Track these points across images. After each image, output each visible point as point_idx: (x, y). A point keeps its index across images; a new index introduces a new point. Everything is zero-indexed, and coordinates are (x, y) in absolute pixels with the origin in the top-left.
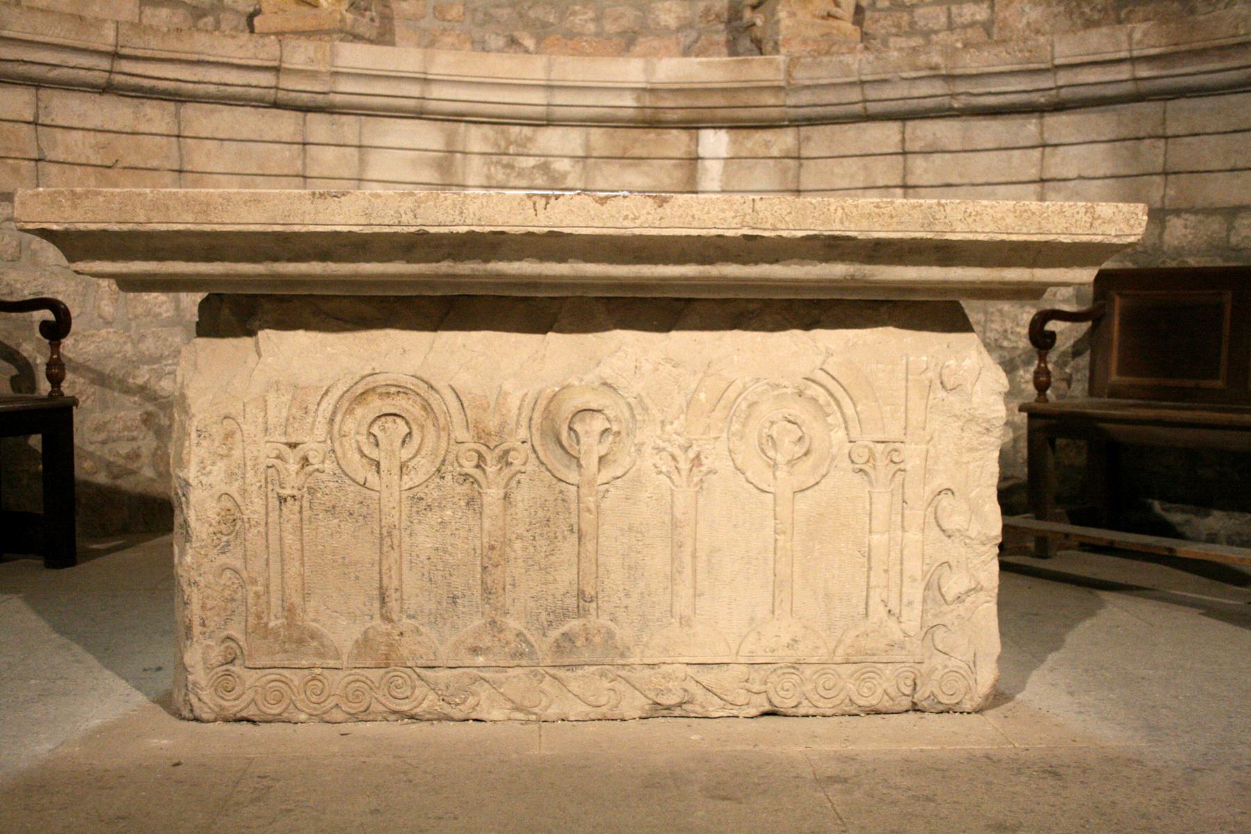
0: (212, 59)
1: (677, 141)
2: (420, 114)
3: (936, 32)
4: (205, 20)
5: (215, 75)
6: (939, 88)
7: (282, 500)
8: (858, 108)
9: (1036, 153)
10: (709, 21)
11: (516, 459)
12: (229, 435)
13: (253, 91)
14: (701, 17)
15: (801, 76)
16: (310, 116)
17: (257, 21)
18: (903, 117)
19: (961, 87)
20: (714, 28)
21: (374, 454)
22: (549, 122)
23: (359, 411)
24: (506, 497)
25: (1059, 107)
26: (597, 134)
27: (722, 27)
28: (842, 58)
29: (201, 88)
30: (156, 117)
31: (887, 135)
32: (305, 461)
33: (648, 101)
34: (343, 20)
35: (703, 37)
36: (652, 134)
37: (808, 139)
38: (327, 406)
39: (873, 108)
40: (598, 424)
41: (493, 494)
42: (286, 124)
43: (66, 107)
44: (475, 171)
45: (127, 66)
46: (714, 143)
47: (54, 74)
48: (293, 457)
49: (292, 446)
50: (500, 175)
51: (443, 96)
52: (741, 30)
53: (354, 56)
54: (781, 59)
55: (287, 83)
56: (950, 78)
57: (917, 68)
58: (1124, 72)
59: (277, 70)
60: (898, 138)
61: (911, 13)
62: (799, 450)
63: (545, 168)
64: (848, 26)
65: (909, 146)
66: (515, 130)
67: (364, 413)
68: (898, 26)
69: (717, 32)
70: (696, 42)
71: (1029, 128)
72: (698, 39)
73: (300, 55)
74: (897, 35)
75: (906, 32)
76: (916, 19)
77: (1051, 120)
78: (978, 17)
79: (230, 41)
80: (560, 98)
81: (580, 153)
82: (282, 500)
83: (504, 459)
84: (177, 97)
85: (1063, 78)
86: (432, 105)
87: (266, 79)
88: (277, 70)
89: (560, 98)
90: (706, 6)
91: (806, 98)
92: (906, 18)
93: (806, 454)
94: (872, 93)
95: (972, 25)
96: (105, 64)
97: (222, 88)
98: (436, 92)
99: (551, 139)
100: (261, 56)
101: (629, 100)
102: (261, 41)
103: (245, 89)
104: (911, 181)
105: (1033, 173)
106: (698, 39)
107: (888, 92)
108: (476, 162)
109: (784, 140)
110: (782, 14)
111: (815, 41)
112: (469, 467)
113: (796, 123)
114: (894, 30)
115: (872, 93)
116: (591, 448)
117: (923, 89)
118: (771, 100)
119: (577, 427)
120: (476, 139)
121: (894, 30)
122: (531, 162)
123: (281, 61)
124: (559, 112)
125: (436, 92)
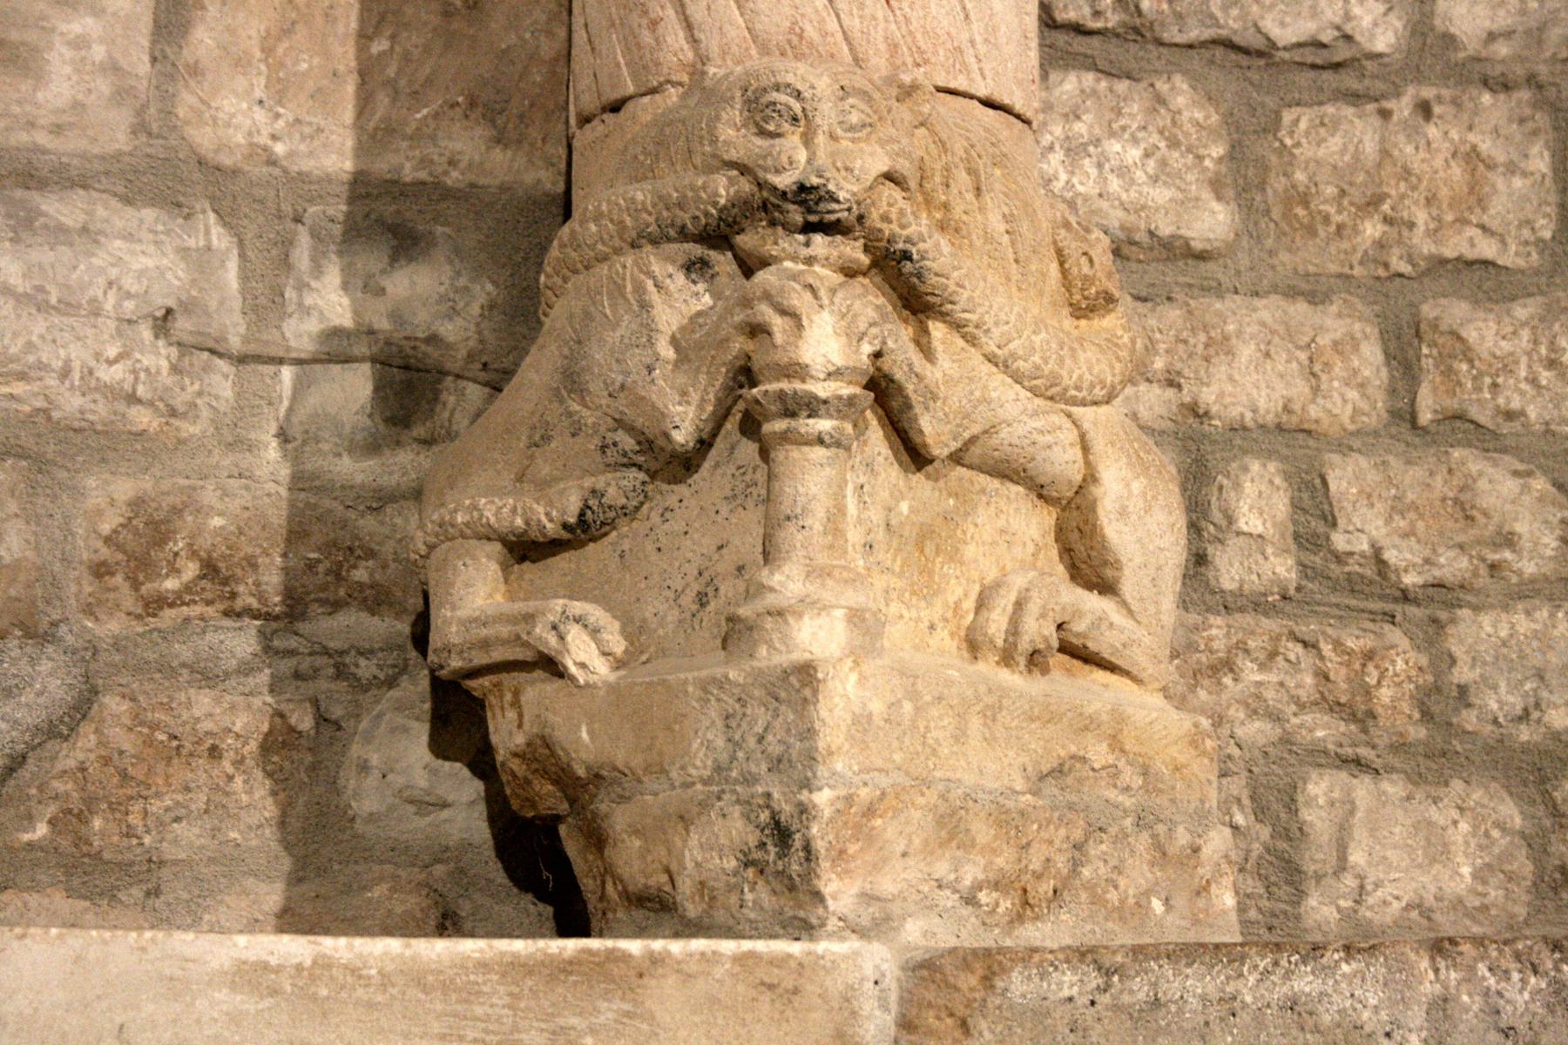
10: (155, 604)
14: (100, 570)
20: (183, 651)
27: (242, 642)
28: (1305, 983)
35: (113, 704)
52: (366, 669)
61: (1433, 634)
68: (1361, 716)
69: (207, 675)
70: (57, 730)
72: (82, 707)
74: (1358, 765)
75: (1401, 747)
76: (1463, 673)
90: (137, 503)
106: (82, 707)
111: (1008, 821)
114: (1324, 730)
121: (1324, 730)
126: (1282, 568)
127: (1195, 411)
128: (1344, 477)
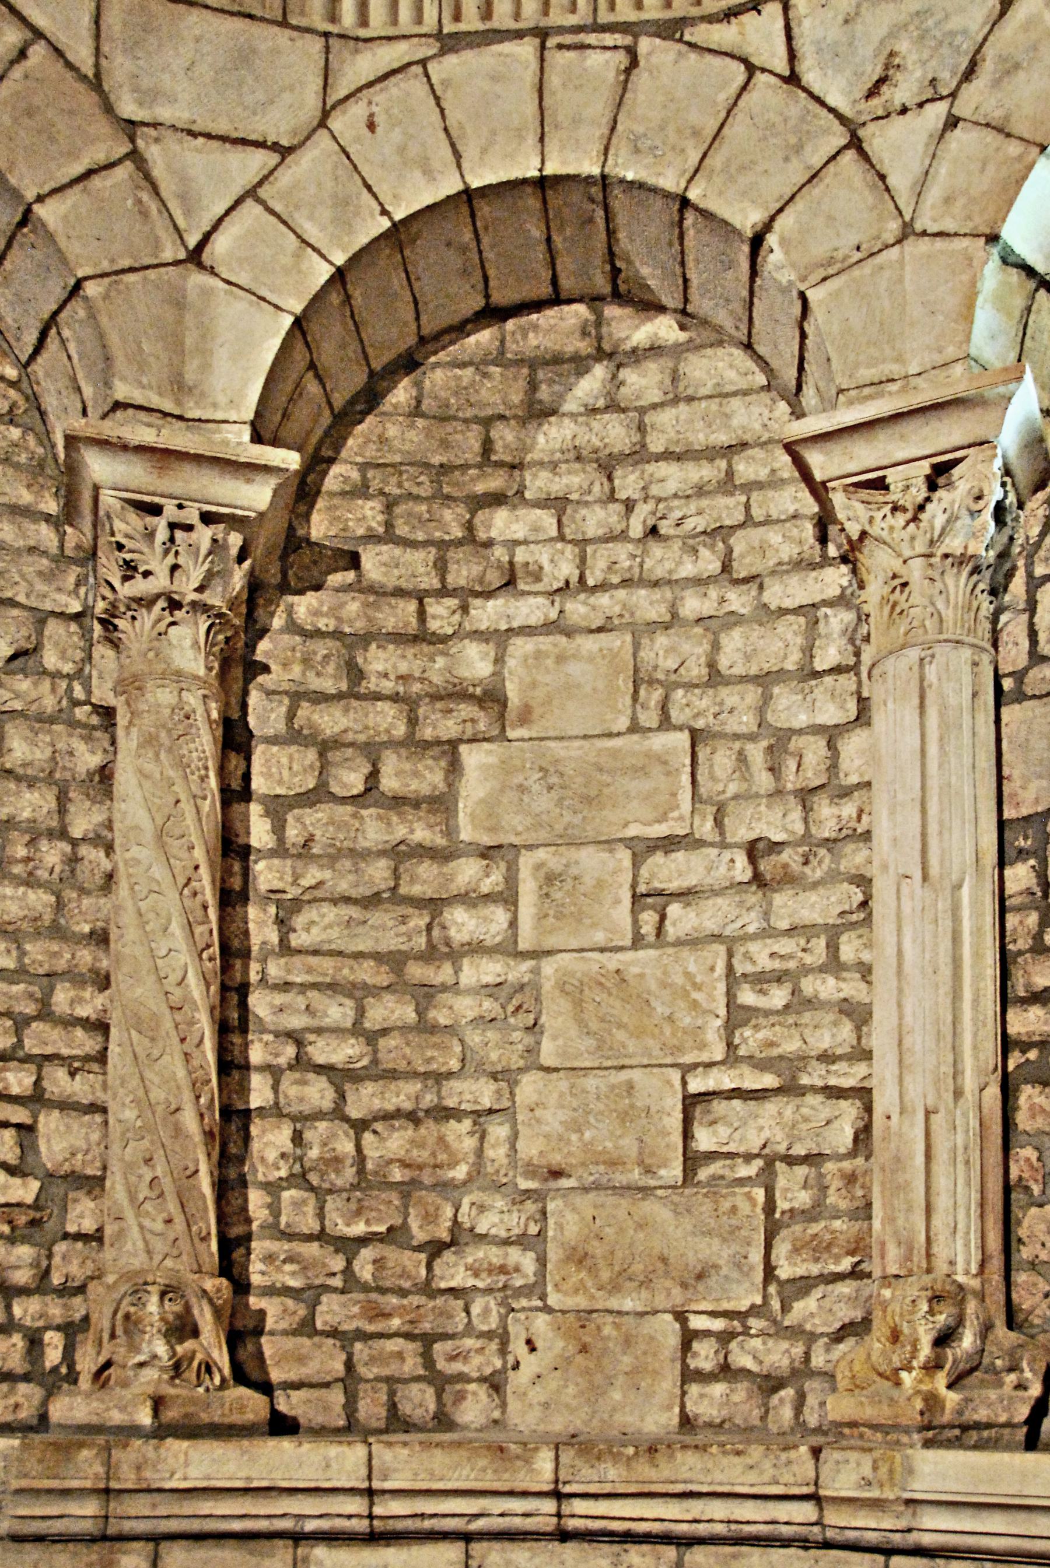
0: (705, 1489)
4: (783, 1393)
5: (718, 1509)
29: (702, 1529)
34: (932, 1401)
59: (814, 1498)
79: (736, 1460)
97: (733, 1527)
100: (787, 1478)
102: (784, 1456)
103: (771, 1527)
123: (816, 1484)
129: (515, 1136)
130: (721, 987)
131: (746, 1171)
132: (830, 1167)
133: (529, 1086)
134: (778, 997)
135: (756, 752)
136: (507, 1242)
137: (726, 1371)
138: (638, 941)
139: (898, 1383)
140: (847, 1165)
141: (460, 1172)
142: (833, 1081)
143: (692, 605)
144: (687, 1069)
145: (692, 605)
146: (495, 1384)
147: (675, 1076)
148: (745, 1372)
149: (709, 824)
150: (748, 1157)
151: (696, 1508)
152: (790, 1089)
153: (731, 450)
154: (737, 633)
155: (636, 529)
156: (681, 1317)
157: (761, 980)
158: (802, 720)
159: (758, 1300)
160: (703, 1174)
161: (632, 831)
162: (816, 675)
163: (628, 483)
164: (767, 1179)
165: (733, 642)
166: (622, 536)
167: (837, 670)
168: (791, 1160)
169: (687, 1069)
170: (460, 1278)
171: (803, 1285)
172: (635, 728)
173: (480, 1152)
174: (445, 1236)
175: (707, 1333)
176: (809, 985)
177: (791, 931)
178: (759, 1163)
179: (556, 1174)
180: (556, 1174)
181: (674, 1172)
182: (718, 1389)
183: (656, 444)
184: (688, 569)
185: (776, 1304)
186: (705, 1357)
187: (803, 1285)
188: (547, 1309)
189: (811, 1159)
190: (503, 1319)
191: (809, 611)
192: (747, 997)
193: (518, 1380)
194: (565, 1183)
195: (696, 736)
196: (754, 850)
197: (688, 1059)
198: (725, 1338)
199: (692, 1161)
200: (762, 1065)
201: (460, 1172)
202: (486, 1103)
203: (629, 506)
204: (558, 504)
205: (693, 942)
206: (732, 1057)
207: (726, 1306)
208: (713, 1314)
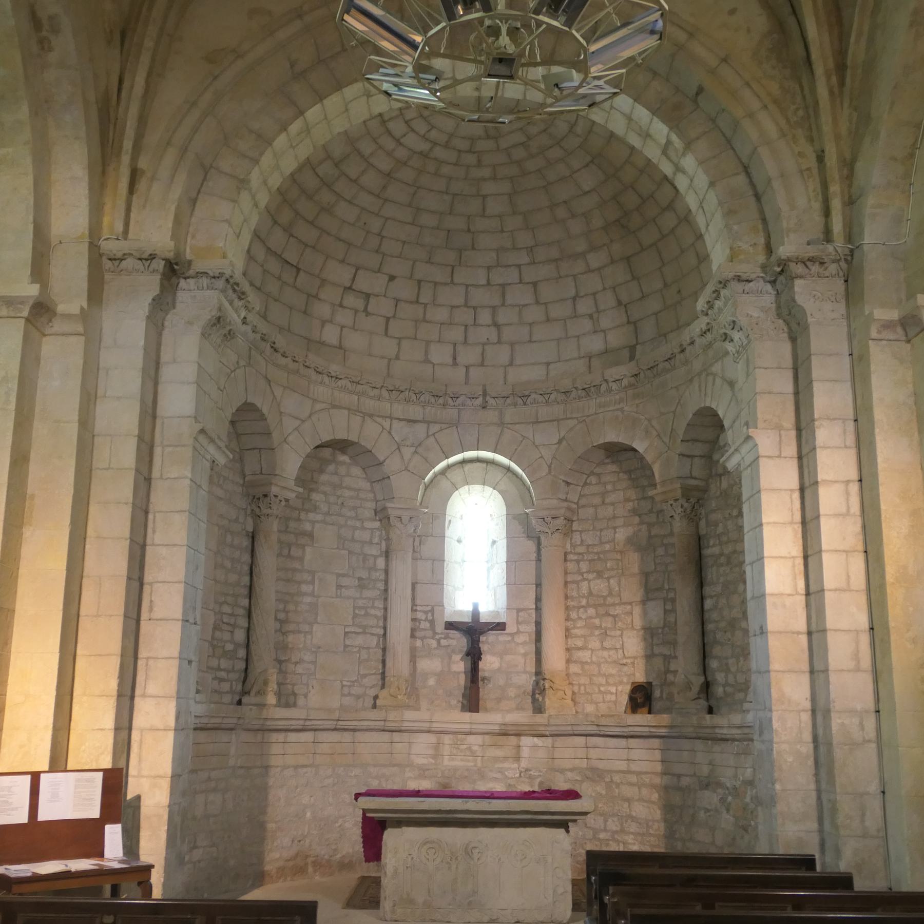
1: (513, 740)
2: (429, 732)
3: (599, 703)
5: (366, 723)
6: (595, 728)
7: (407, 867)
8: (571, 733)
9: (627, 750)
11: (459, 858)
12: (396, 852)
13: (376, 727)
15: (552, 722)
16: (394, 733)
17: (377, 701)
18: (586, 735)
19: (602, 728)
21: (427, 857)
22: (471, 733)
23: (425, 847)
24: (457, 867)
25: (632, 737)
26: (487, 737)
30: (347, 736)
31: (581, 741)
32: (412, 858)
33: (503, 727)
36: (505, 737)
37: (556, 741)
38: (418, 844)
39: (576, 733)
40: (477, 850)
41: (453, 867)
42: (386, 736)
43: (323, 736)
44: (446, 750)
45: (340, 723)
46: (526, 741)
47: (321, 727)
48: (410, 858)
49: (410, 855)
50: (455, 752)
51: (436, 726)
53: (409, 715)
54: (546, 715)
55: (388, 724)
56: (598, 725)
57: (588, 721)
58: (647, 729)
59: (385, 720)
60: (585, 742)
62: (523, 857)
63: (469, 749)
64: (569, 701)
65: (588, 745)
66: (460, 736)
67: (426, 847)
71: (622, 742)
73: (392, 716)
77: (631, 741)
78: (612, 699)
80: (474, 727)
81: (481, 744)
82: (407, 867)
83: (456, 859)
84: (354, 730)
85: (631, 729)
86: (433, 729)
87: (382, 723)
88: (385, 720)
89: (474, 727)
91: (554, 728)
92: (589, 697)
93: (525, 858)
94: (575, 728)
95: (610, 701)
96: (335, 723)
98: (435, 725)
99: (471, 739)
101: (497, 727)
104: (589, 757)
105: (625, 757)
107: (579, 728)
108: (447, 747)
109: (548, 741)
110: (547, 700)
112: (449, 860)
113: (551, 735)
115: (575, 728)
116: (476, 856)
117: (590, 728)
118: (542, 728)
119: (473, 851)
120: (447, 739)
122: (465, 747)
124: (474, 731)
125: (435, 725)
126: (584, 692)
127: (579, 683)
128: (587, 687)
129: (312, 638)
130: (352, 609)
131: (355, 650)
132: (371, 650)
133: (315, 627)
134: (363, 612)
135: (361, 558)
136: (309, 663)
137: (349, 694)
138: (337, 597)
139: (396, 697)
140: (375, 650)
141: (301, 646)
142: (372, 632)
143: (349, 523)
144: (346, 626)
145: (349, 523)
146: (306, 696)
147: (343, 627)
148: (354, 695)
149: (351, 572)
150: (356, 647)
151: (362, 723)
152: (364, 633)
153: (359, 490)
154: (358, 531)
155: (340, 502)
156: (341, 682)
157: (360, 608)
158: (369, 552)
159: (356, 678)
160: (347, 649)
161: (336, 571)
162: (372, 543)
163: (339, 493)
164: (359, 652)
165: (357, 533)
166: (336, 504)
167: (377, 544)
168: (364, 648)
169: (346, 626)
170: (300, 671)
171: (365, 676)
172: (338, 548)
173: (305, 641)
174: (298, 661)
175: (346, 686)
176: (368, 610)
177: (365, 598)
178: (357, 649)
179: (319, 647)
180: (319, 647)
181: (342, 649)
182: (348, 698)
183: (344, 485)
184: (349, 514)
185: (360, 679)
186: (346, 691)
187: (365, 676)
188: (316, 679)
189: (368, 648)
190: (308, 681)
191: (372, 529)
192: (357, 611)
193: (310, 695)
194: (321, 650)
195: (350, 553)
196: (360, 579)
197: (345, 624)
198: (350, 686)
199: (346, 646)
200: (360, 627)
201: (301, 646)
202: (307, 630)
203: (339, 497)
204: (325, 493)
205: (348, 598)
206: (353, 625)
207: (351, 680)
208: (348, 681)
